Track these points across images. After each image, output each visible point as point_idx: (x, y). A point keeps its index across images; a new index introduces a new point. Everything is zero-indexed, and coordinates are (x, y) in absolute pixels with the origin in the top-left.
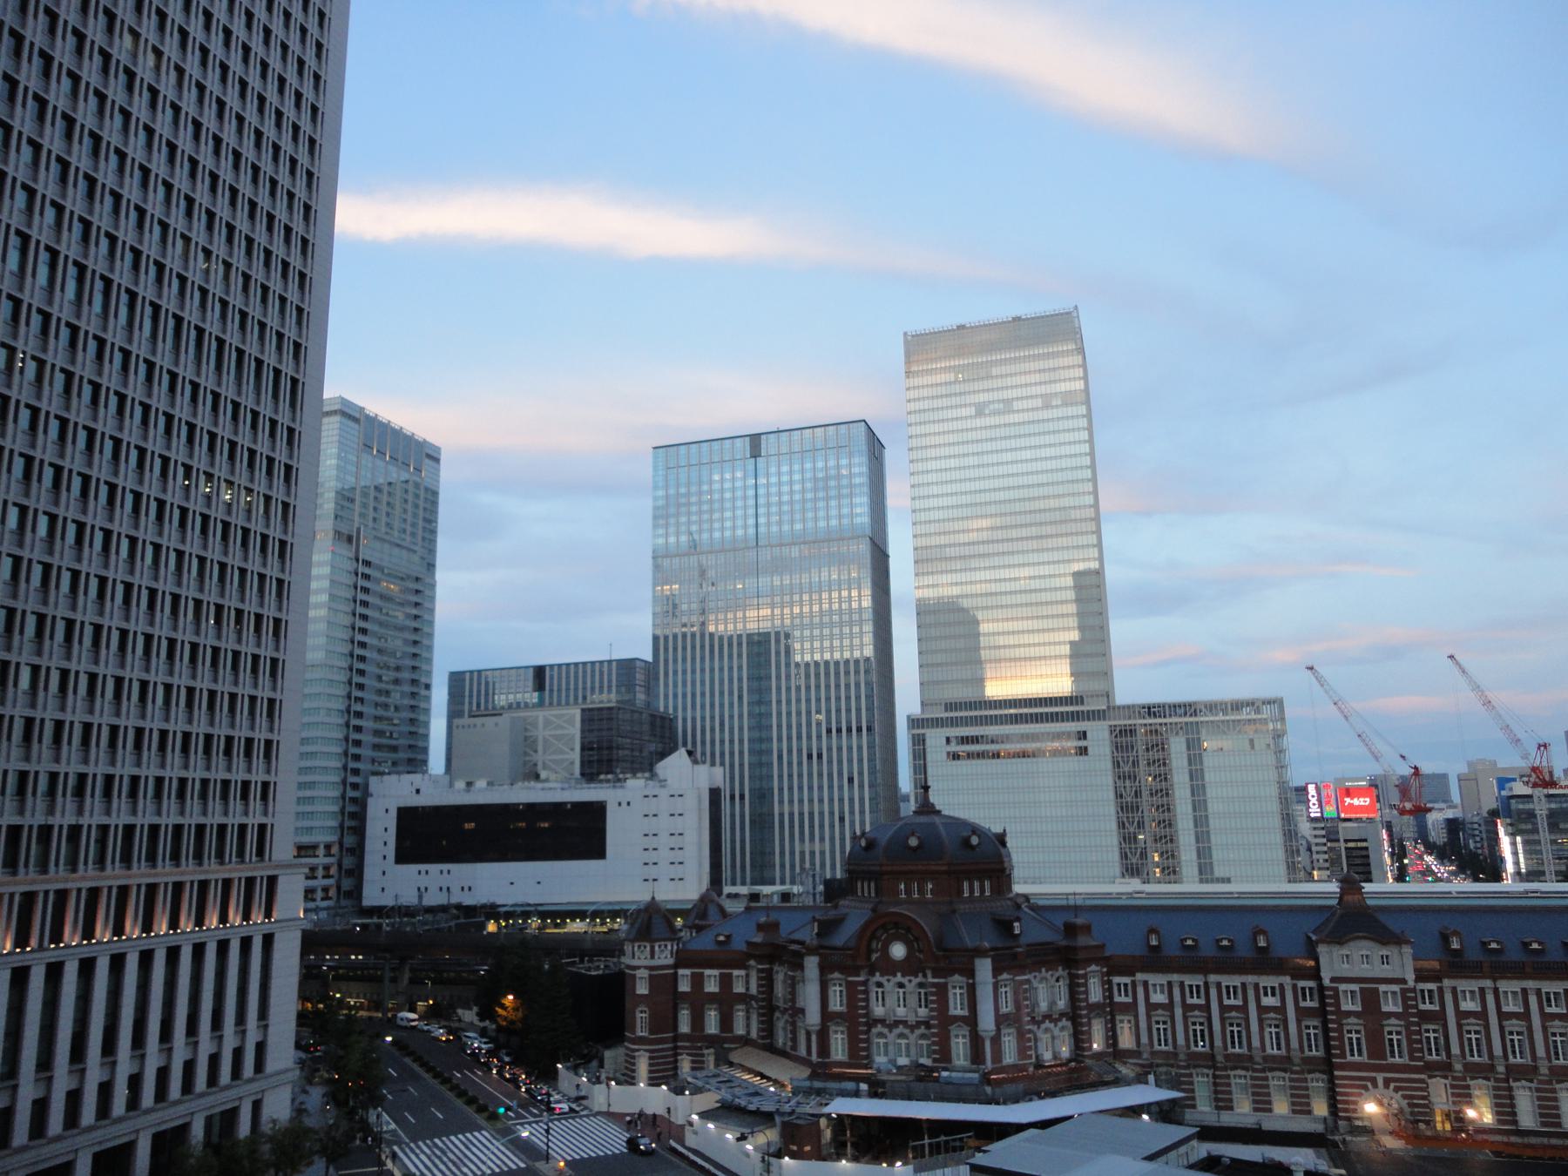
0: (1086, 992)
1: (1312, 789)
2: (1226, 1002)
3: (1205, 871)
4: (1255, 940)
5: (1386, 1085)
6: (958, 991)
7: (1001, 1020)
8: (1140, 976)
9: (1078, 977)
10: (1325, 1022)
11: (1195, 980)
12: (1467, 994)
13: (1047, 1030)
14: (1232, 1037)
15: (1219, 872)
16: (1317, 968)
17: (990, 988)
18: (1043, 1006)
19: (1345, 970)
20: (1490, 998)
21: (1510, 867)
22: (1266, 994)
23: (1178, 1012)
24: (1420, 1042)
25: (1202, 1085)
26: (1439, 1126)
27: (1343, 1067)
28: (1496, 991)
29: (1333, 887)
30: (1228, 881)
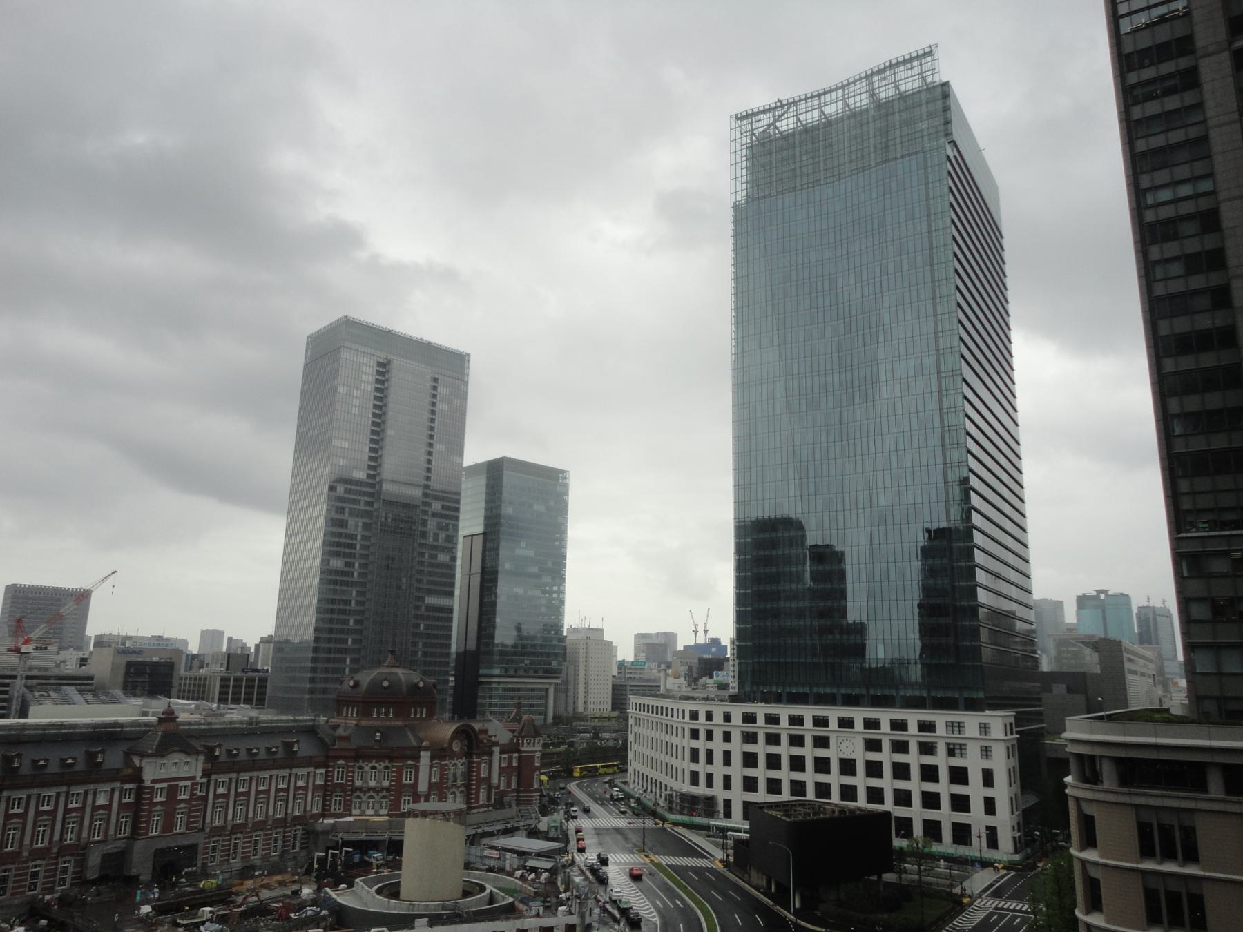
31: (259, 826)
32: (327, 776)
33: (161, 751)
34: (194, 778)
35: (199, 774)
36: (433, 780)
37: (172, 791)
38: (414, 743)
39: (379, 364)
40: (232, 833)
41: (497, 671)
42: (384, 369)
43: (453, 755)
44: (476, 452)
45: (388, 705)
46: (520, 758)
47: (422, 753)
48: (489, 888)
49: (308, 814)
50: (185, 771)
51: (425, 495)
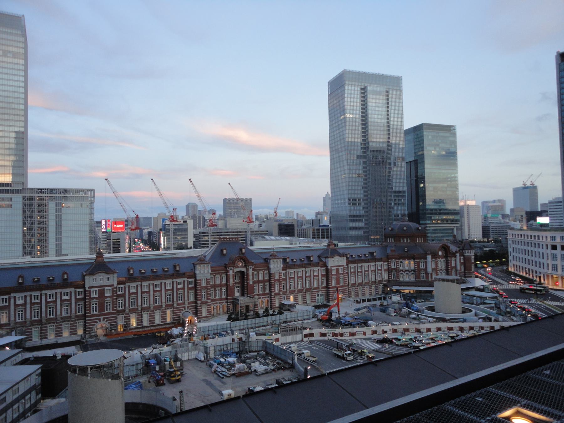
1: (103, 222)
2: (49, 300)
3: (58, 252)
4: (63, 277)
5: (103, 320)
8: (12, 295)
10: (85, 303)
11: (38, 293)
12: (133, 287)
14: (50, 312)
15: (64, 252)
16: (84, 284)
19: (95, 284)
20: (139, 288)
21: (162, 246)
22: (64, 295)
23: (28, 306)
24: (116, 304)
25: (35, 332)
26: (119, 330)
28: (141, 285)
29: (94, 256)
30: (67, 255)
31: (367, 284)
32: (388, 265)
33: (332, 256)
34: (343, 266)
36: (433, 267)
37: (337, 270)
38: (422, 252)
39: (362, 89)
40: (358, 286)
41: (428, 222)
42: (364, 91)
43: (439, 257)
44: (409, 124)
45: (407, 237)
46: (464, 259)
47: (428, 256)
48: (474, 311)
50: (340, 264)
51: (388, 146)
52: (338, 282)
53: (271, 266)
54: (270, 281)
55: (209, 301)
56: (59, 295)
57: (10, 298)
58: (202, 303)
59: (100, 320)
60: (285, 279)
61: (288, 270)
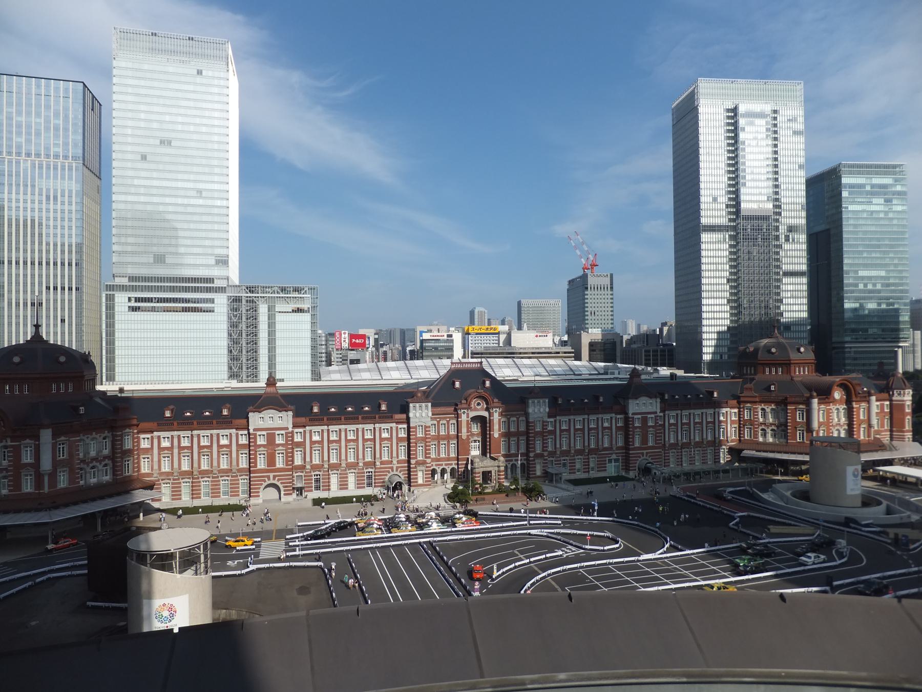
0: (121, 444)
6: (29, 449)
7: (56, 464)
8: (156, 434)
9: (117, 436)
13: (93, 468)
17: (50, 446)
18: (93, 453)
20: (325, 434)
23: (176, 451)
27: (255, 472)
31: (698, 445)
32: (739, 414)
34: (656, 413)
35: (658, 411)
37: (644, 420)
46: (891, 406)
48: (885, 503)
49: (729, 439)
52: (644, 440)
53: (530, 410)
54: (527, 433)
55: (428, 460)
56: (215, 439)
57: (152, 438)
58: (419, 463)
59: (269, 478)
60: (553, 432)
61: (558, 418)
